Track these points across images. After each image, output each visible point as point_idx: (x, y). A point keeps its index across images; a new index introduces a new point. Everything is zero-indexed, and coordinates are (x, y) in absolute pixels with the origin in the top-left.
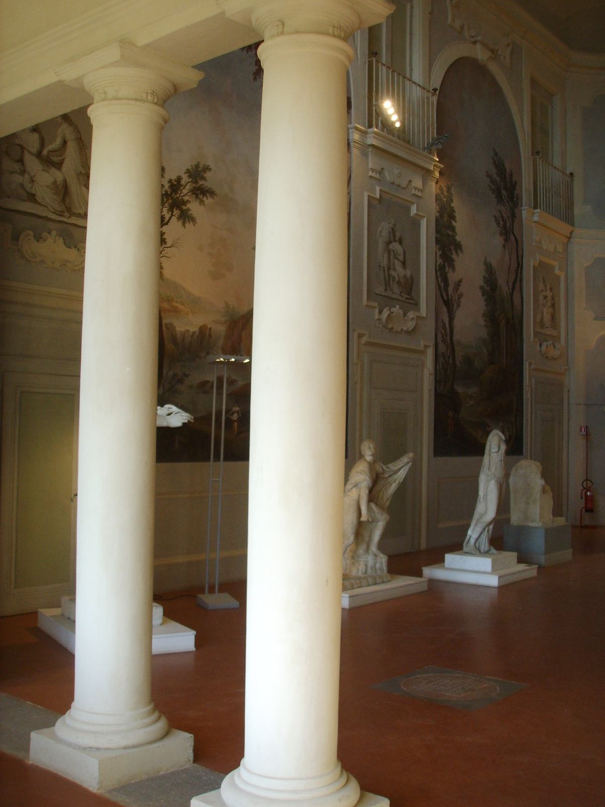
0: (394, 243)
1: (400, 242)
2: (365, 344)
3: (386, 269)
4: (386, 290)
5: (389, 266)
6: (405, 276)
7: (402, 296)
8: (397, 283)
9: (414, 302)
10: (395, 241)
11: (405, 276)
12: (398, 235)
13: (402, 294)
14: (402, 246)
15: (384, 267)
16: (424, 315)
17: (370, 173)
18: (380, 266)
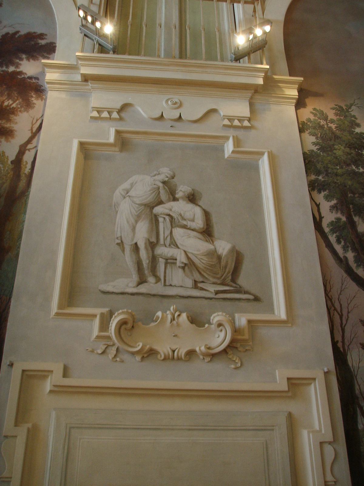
0: (173, 204)
1: (192, 198)
2: (51, 391)
3: (142, 245)
4: (142, 281)
5: (154, 240)
6: (213, 254)
7: (202, 289)
8: (183, 268)
9: (251, 297)
10: (175, 199)
11: (213, 254)
12: (182, 190)
13: (200, 285)
14: (199, 206)
15: (136, 248)
16: (283, 316)
17: (95, 114)
18: (121, 244)
